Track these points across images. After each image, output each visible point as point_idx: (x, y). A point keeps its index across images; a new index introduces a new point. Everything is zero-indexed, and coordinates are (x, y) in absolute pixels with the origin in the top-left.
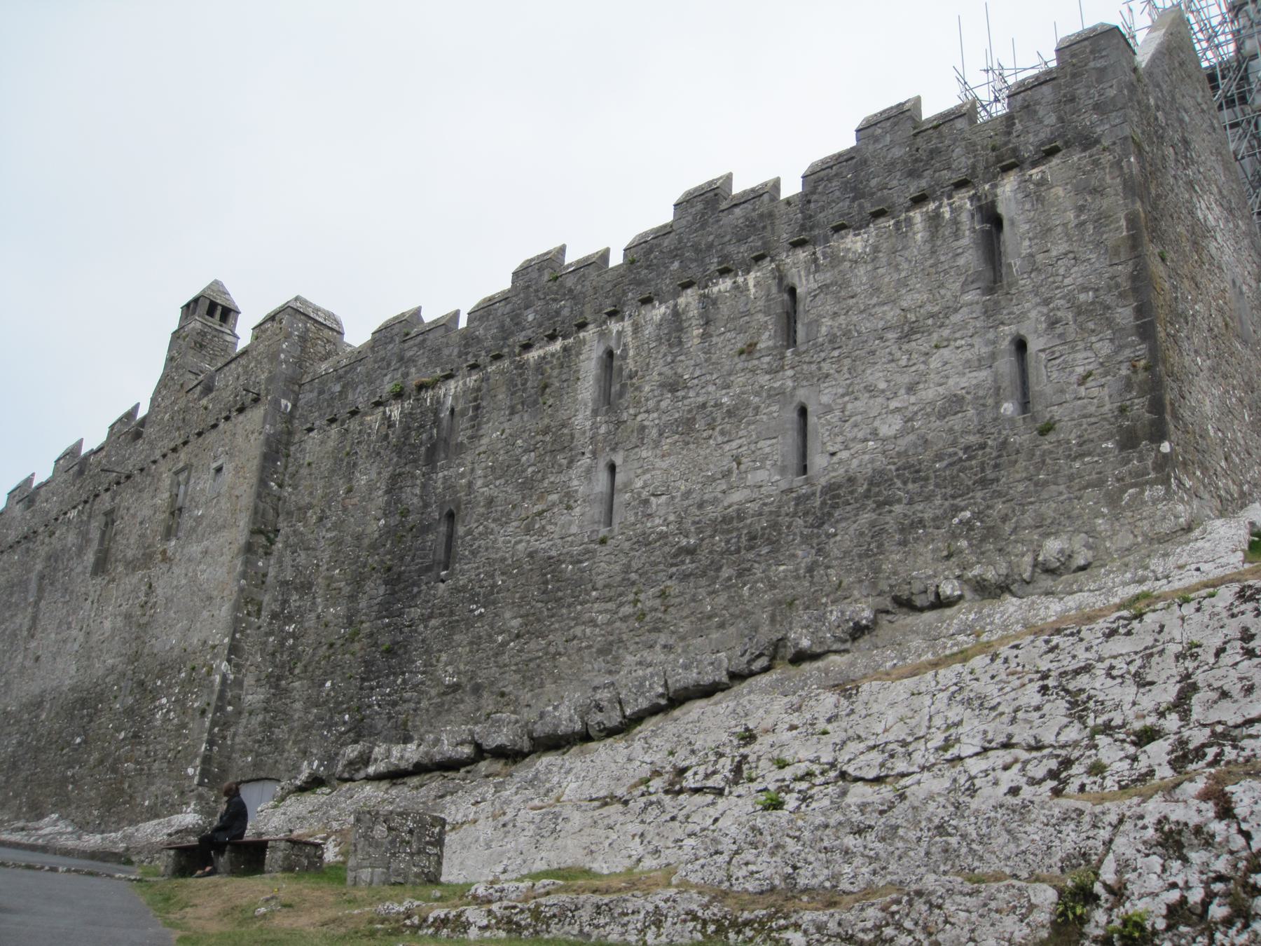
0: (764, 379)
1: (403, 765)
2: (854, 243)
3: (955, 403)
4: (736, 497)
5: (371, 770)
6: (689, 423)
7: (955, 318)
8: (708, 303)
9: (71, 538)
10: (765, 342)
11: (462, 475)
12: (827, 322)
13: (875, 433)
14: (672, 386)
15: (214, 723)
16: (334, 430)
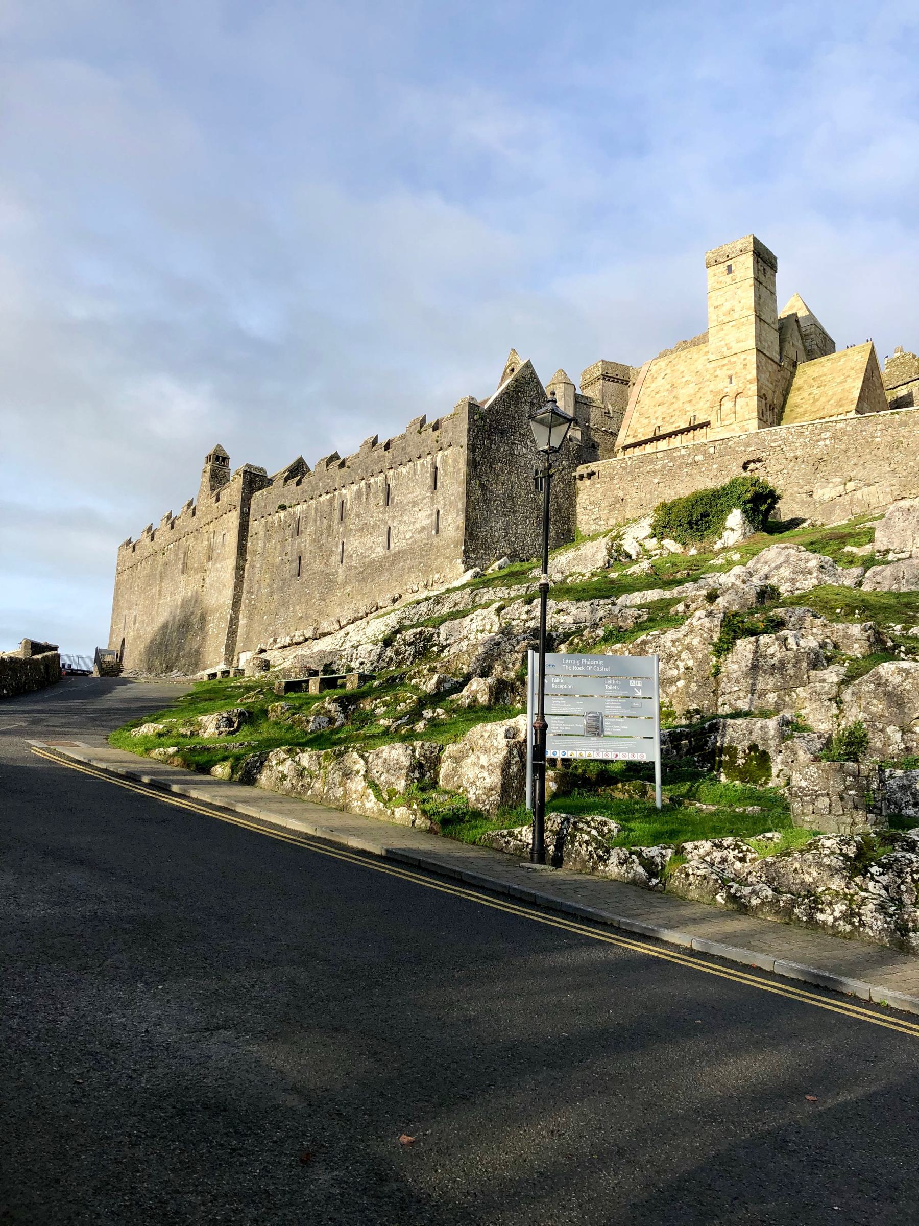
0: (381, 516)
1: (286, 644)
2: (404, 470)
3: (423, 528)
4: (373, 555)
5: (277, 646)
6: (363, 529)
7: (425, 501)
8: (368, 486)
9: (172, 557)
10: (382, 503)
11: (303, 542)
12: (396, 497)
13: (405, 537)
14: (358, 515)
15: (229, 633)
16: (263, 520)
